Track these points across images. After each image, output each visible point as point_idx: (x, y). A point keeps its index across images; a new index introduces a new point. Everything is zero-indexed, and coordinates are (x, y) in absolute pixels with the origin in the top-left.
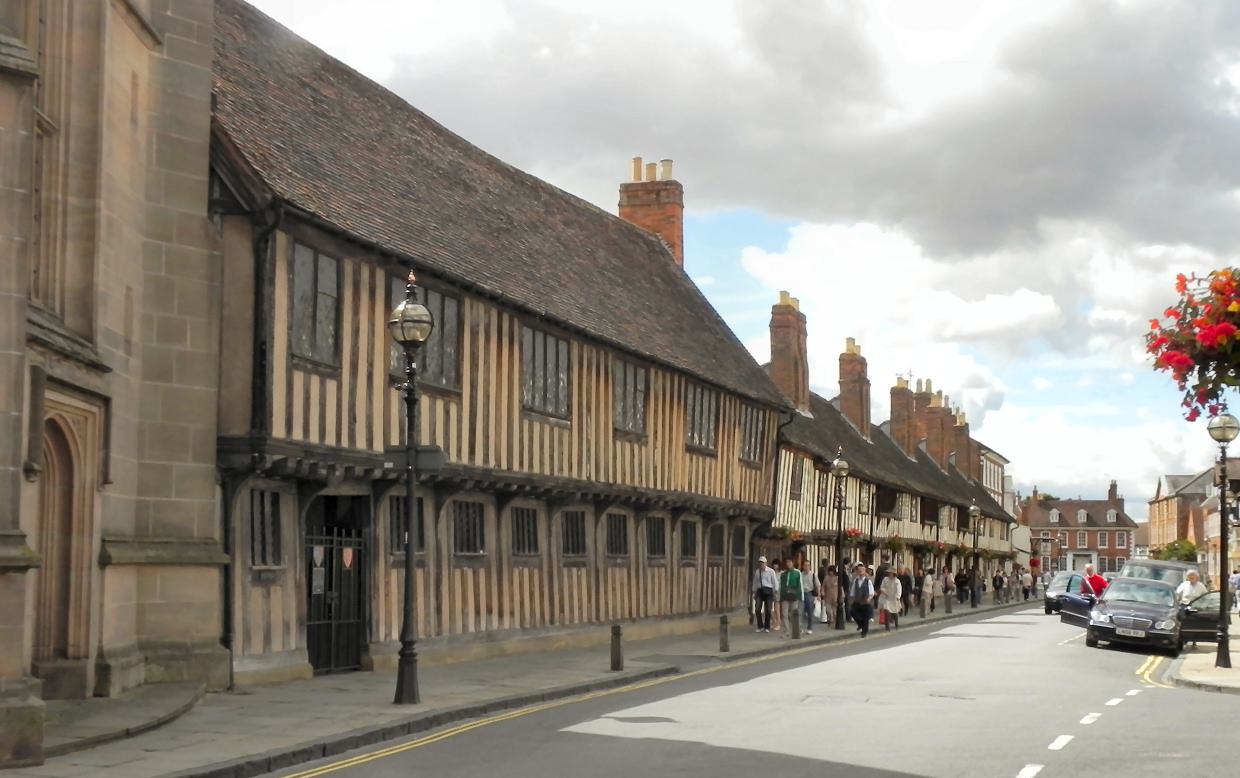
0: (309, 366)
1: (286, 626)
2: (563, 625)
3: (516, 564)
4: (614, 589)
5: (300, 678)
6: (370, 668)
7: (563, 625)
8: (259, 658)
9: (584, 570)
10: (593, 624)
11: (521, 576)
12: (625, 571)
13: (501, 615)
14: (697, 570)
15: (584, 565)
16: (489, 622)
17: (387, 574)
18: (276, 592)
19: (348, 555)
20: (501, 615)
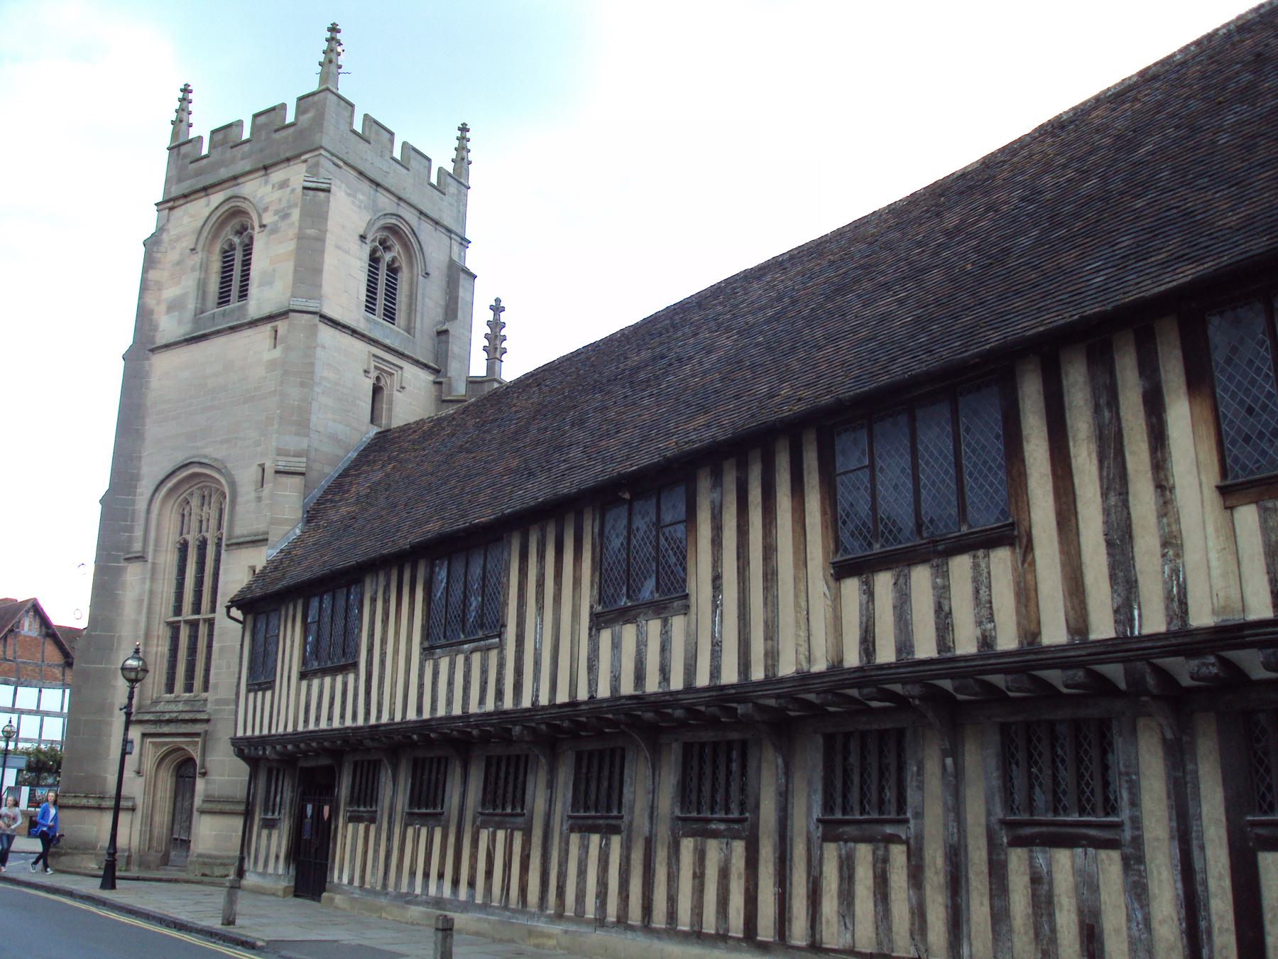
0: (257, 687)
1: (277, 857)
2: (622, 921)
3: (484, 825)
4: (699, 877)
5: (274, 894)
6: (319, 901)
7: (560, 916)
8: (260, 874)
9: (616, 841)
10: (632, 928)
11: (493, 839)
12: (739, 847)
13: (456, 883)
14: (1134, 862)
15: (616, 830)
16: (440, 887)
17: (345, 827)
18: (275, 833)
19: (326, 809)
20: (456, 883)
